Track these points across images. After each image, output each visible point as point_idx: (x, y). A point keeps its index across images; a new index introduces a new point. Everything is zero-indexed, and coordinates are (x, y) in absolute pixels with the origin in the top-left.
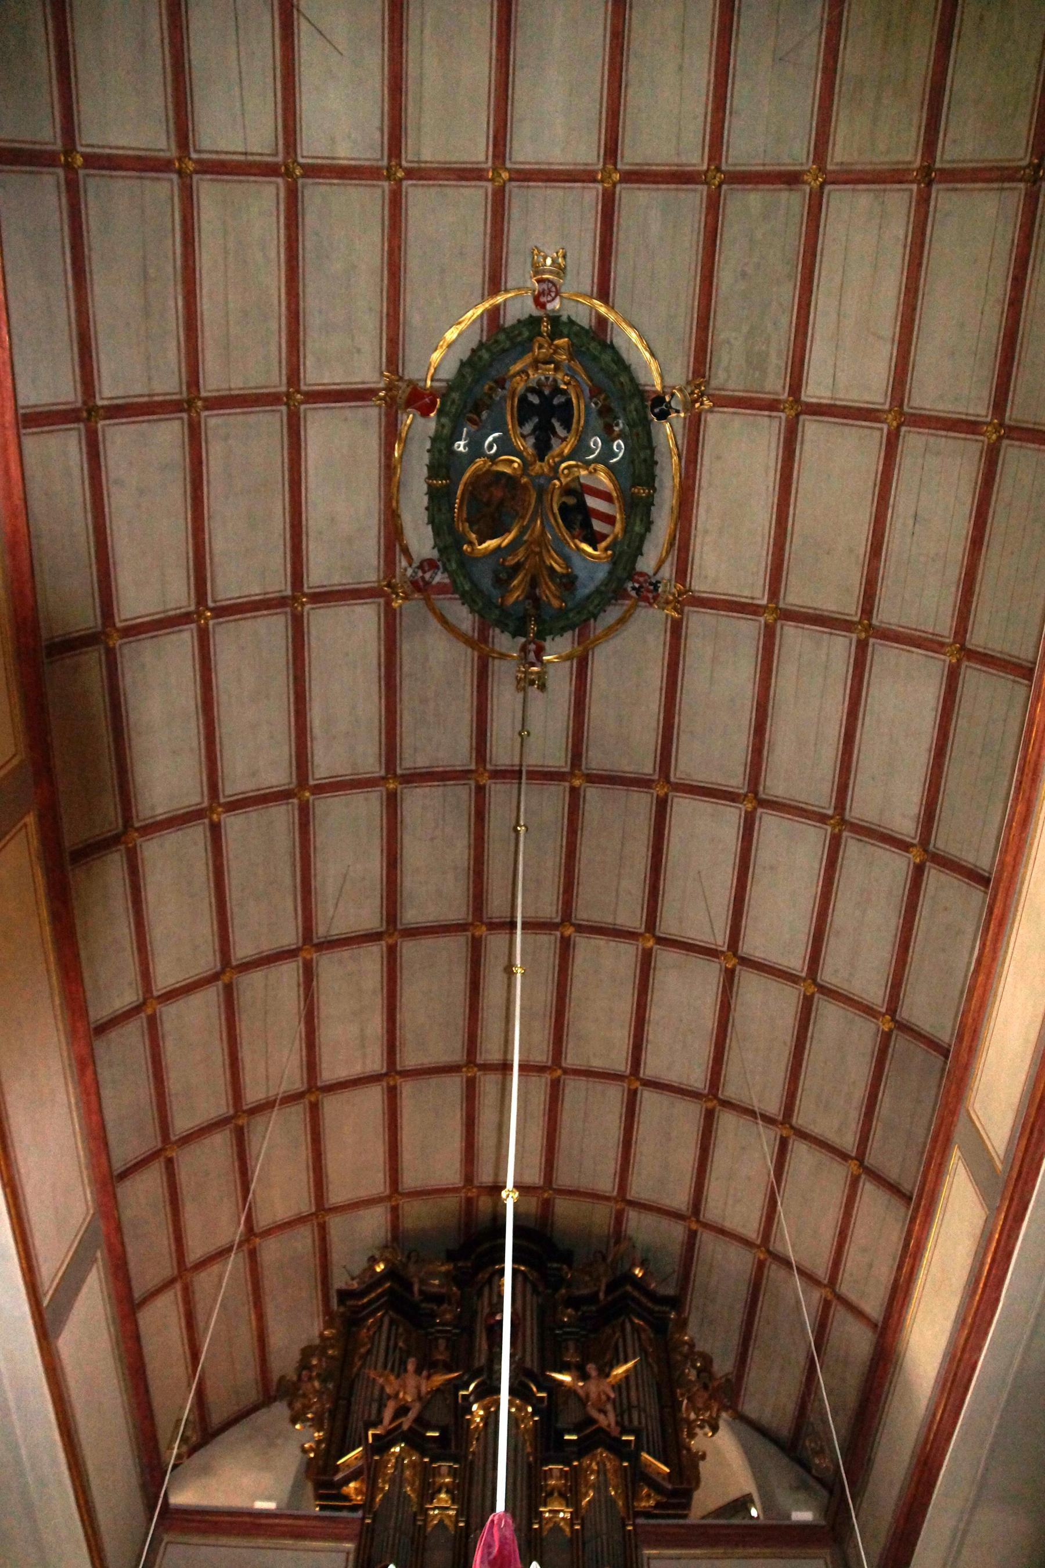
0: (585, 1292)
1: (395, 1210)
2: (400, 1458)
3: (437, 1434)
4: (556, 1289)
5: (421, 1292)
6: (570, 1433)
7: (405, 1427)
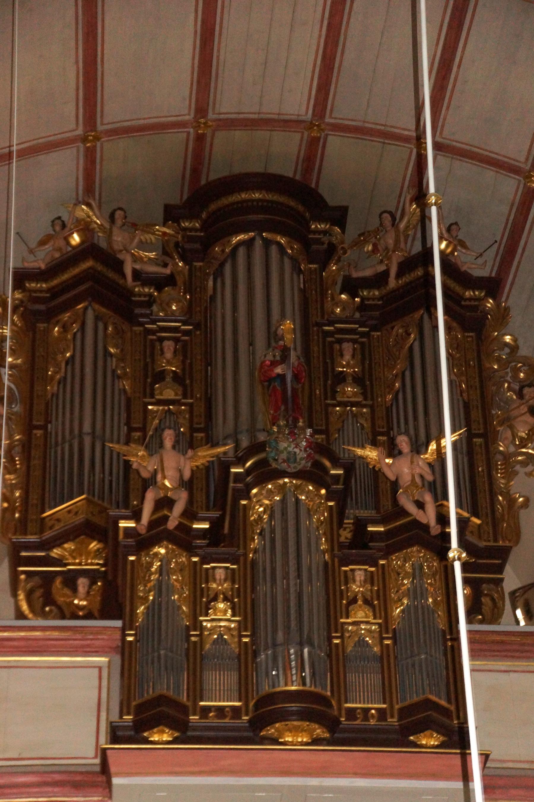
0: (368, 273)
1: (90, 157)
2: (165, 561)
3: (206, 526)
4: (324, 266)
5: (136, 275)
6: (375, 523)
7: (172, 524)
